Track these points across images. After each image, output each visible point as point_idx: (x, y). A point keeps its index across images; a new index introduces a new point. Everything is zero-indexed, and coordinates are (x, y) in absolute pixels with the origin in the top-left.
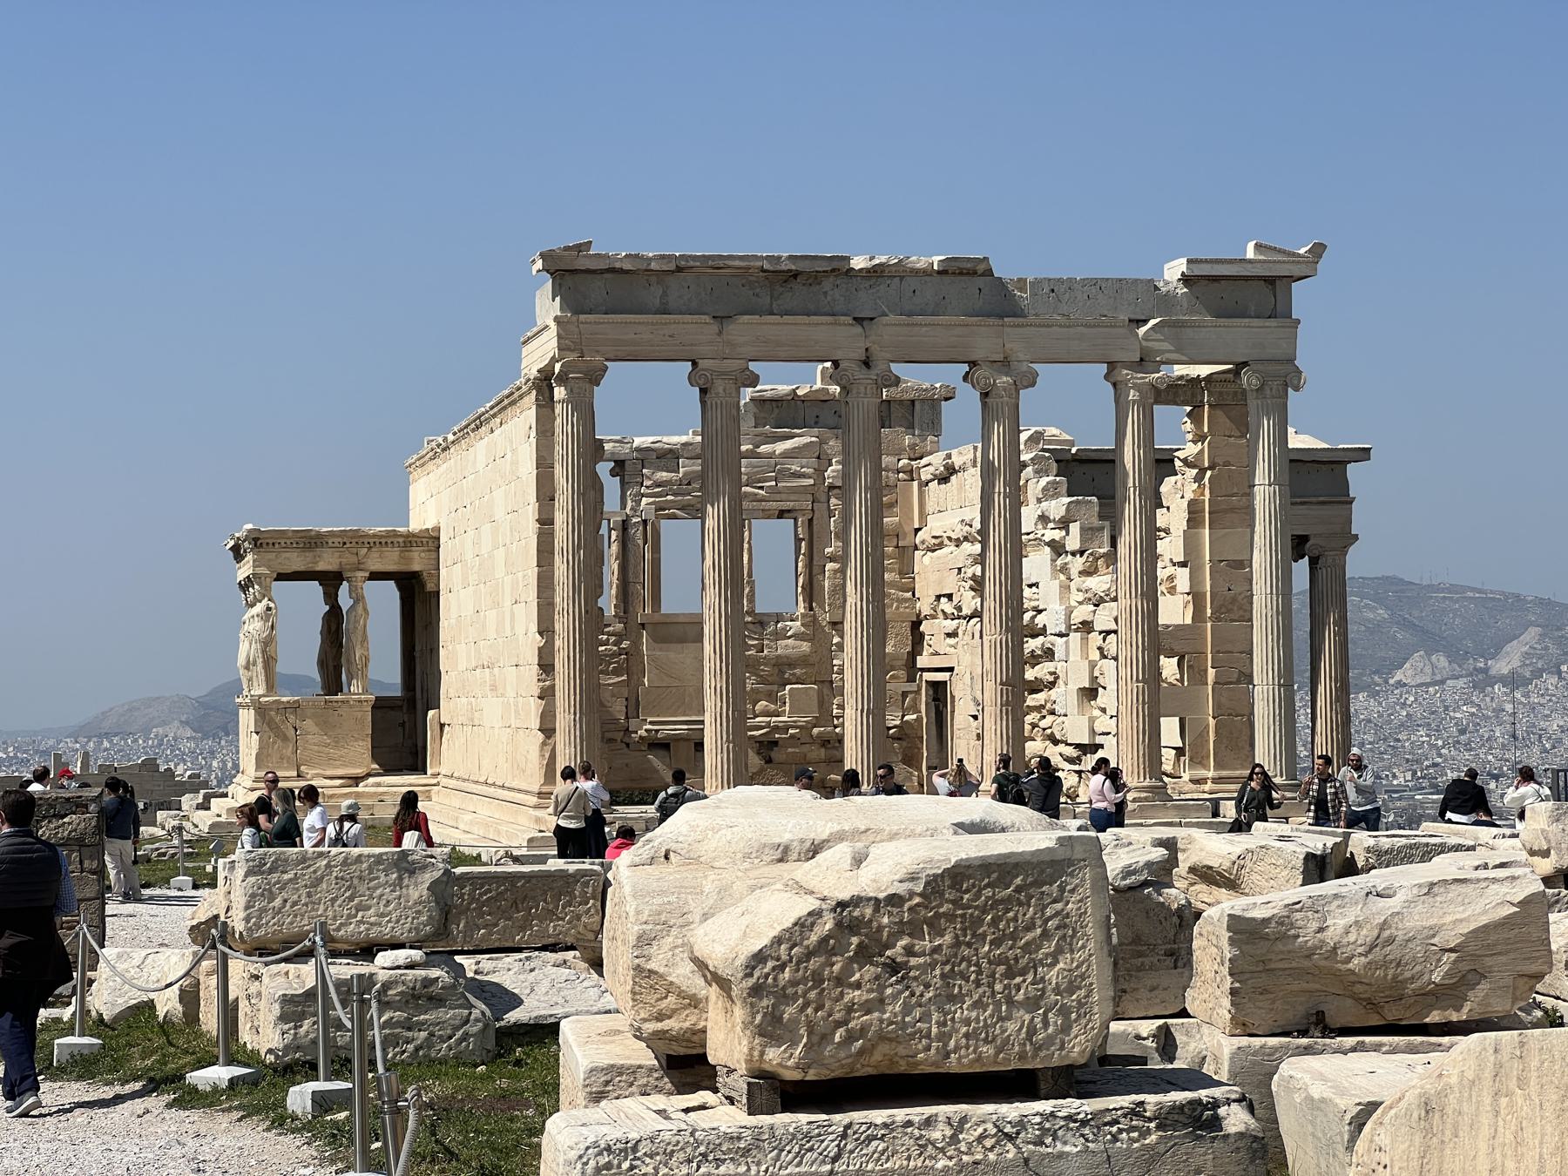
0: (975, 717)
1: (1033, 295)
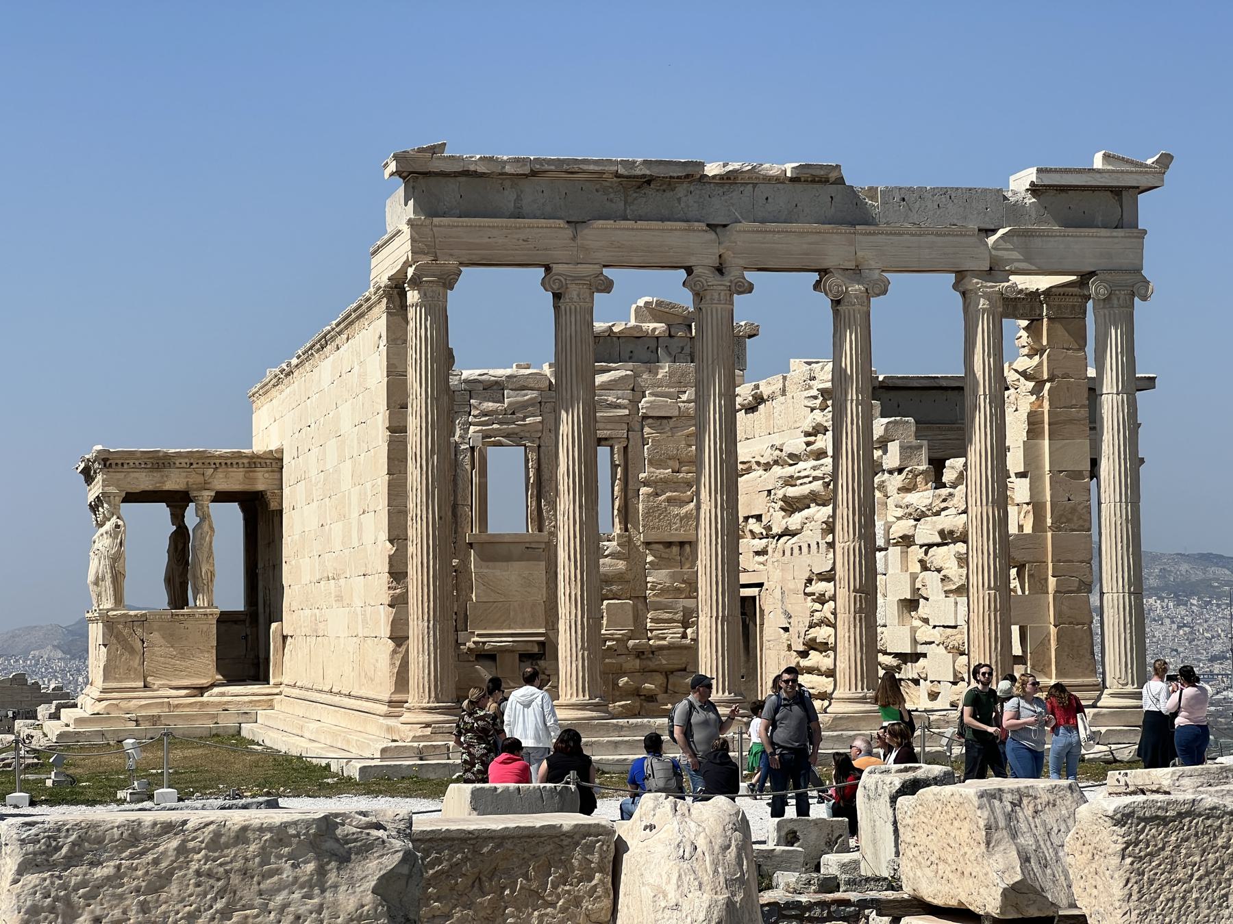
0: (786, 630)
1: (884, 203)
